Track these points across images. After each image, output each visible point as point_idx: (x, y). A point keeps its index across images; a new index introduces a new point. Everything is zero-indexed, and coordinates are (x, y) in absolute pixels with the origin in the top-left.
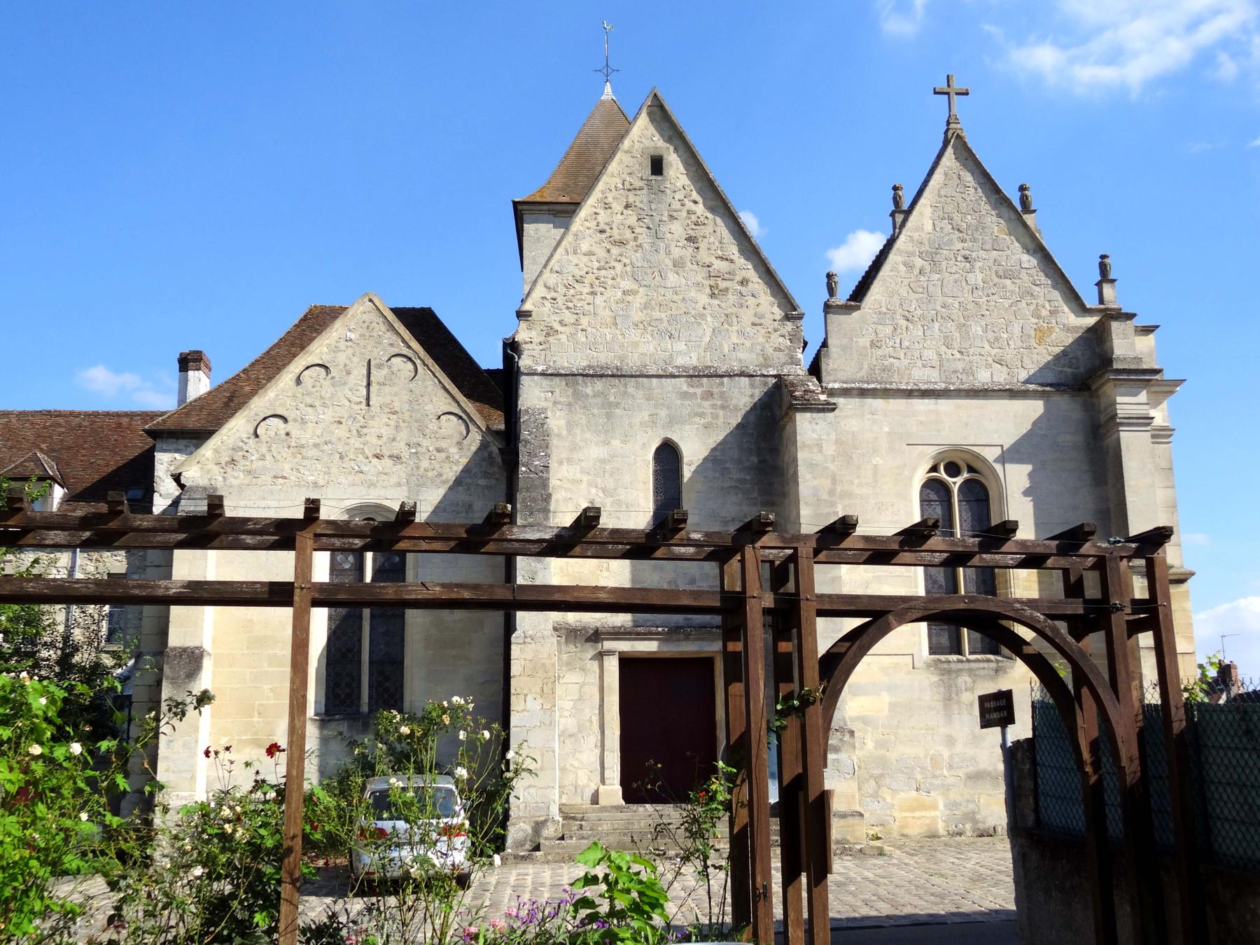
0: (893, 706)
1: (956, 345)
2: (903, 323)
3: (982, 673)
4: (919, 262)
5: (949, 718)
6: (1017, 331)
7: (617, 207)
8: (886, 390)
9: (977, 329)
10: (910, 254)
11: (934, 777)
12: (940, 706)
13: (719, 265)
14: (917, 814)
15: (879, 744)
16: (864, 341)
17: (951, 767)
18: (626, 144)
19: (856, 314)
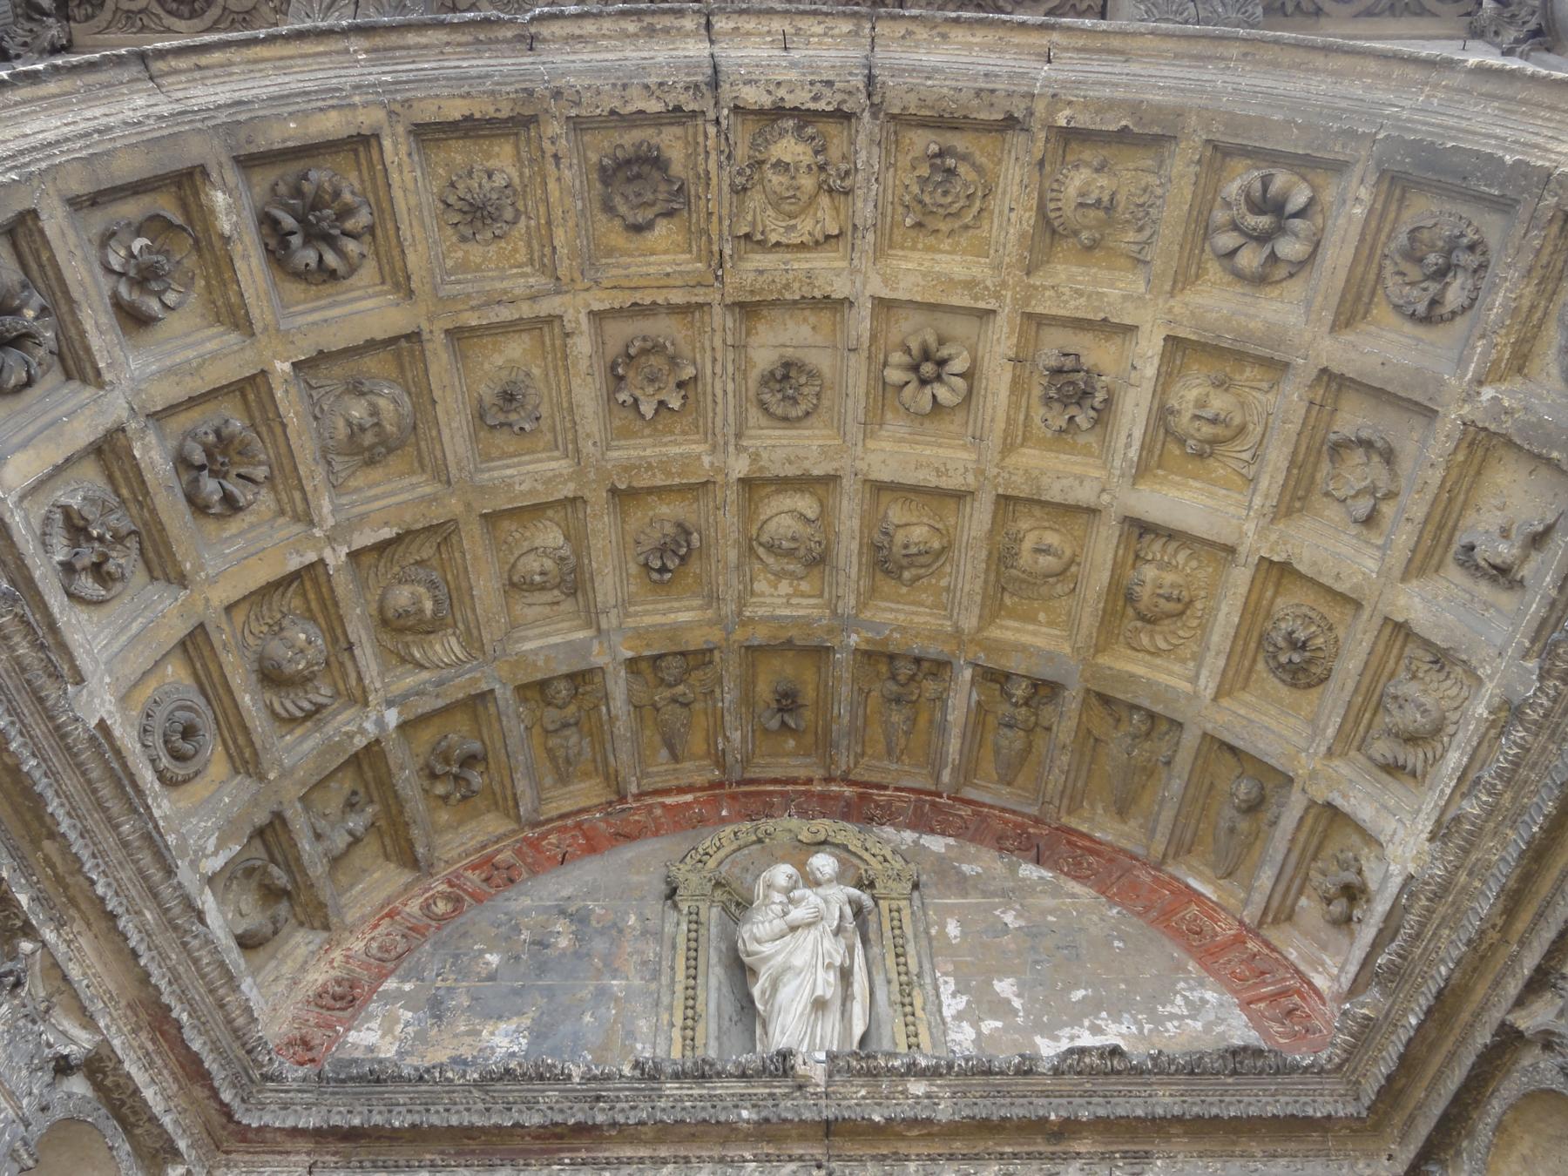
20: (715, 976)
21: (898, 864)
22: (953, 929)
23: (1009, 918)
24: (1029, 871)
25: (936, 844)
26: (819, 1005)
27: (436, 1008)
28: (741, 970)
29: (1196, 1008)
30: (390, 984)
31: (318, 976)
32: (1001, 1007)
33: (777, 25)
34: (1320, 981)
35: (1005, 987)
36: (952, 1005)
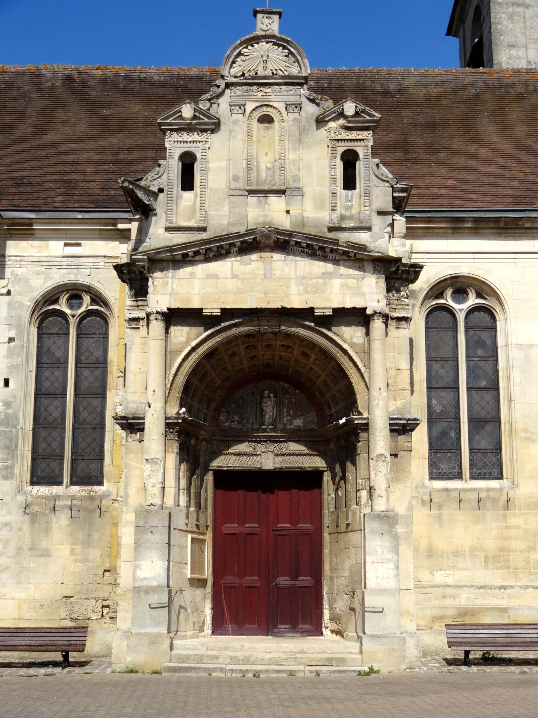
20: (259, 408)
21: (281, 389)
22: (286, 402)
23: (293, 400)
24: (297, 391)
25: (286, 385)
26: (270, 418)
27: (228, 413)
28: (262, 410)
29: (311, 415)
30: (223, 410)
31: (214, 406)
32: (290, 415)
33: (268, 318)
34: (327, 412)
35: (291, 412)
36: (285, 414)
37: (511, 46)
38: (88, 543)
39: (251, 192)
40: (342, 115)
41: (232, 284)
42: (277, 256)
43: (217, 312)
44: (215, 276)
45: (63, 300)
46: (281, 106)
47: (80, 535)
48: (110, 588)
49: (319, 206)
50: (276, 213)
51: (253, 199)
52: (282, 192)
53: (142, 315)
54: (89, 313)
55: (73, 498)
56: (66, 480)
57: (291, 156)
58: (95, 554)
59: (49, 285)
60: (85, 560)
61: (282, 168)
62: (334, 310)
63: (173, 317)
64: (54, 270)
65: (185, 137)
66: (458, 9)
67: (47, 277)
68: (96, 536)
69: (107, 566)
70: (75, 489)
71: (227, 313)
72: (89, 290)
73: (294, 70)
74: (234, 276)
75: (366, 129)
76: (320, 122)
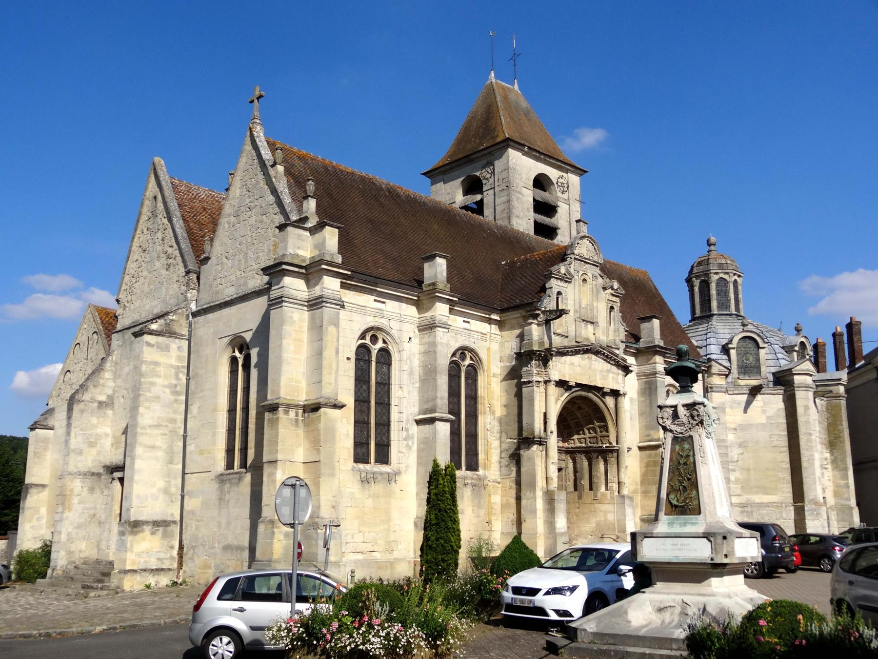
0: (203, 503)
1: (242, 267)
2: (225, 260)
3: (234, 481)
4: (232, 219)
5: (220, 508)
6: (266, 250)
7: (145, 231)
8: (211, 307)
9: (250, 254)
10: (230, 215)
11: (212, 548)
12: (217, 502)
13: (170, 250)
14: (205, 571)
15: (197, 528)
16: (211, 277)
17: (219, 542)
18: (147, 194)
19: (210, 262)
37: (518, 217)
38: (479, 506)
39: (584, 320)
40: (612, 288)
41: (578, 370)
42: (594, 357)
43: (574, 384)
44: (572, 364)
45: (458, 355)
46: (590, 275)
47: (476, 501)
48: (488, 533)
49: (603, 334)
50: (589, 334)
51: (583, 324)
52: (593, 323)
53: (541, 379)
54: (469, 365)
55: (472, 479)
56: (464, 468)
57: (595, 304)
58: (482, 512)
59: (457, 346)
60: (478, 516)
61: (592, 310)
62: (611, 390)
63: (562, 384)
64: (459, 336)
65: (562, 284)
66: (448, 167)
67: (456, 341)
68: (482, 502)
69: (487, 520)
70: (468, 472)
71: (578, 385)
72: (471, 351)
73: (596, 258)
74: (579, 366)
75: (617, 296)
76: (605, 289)
